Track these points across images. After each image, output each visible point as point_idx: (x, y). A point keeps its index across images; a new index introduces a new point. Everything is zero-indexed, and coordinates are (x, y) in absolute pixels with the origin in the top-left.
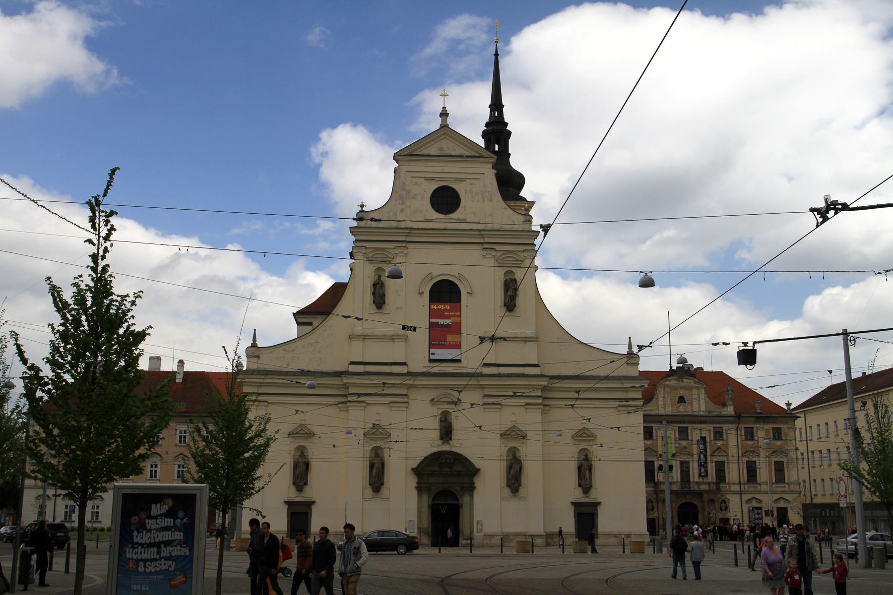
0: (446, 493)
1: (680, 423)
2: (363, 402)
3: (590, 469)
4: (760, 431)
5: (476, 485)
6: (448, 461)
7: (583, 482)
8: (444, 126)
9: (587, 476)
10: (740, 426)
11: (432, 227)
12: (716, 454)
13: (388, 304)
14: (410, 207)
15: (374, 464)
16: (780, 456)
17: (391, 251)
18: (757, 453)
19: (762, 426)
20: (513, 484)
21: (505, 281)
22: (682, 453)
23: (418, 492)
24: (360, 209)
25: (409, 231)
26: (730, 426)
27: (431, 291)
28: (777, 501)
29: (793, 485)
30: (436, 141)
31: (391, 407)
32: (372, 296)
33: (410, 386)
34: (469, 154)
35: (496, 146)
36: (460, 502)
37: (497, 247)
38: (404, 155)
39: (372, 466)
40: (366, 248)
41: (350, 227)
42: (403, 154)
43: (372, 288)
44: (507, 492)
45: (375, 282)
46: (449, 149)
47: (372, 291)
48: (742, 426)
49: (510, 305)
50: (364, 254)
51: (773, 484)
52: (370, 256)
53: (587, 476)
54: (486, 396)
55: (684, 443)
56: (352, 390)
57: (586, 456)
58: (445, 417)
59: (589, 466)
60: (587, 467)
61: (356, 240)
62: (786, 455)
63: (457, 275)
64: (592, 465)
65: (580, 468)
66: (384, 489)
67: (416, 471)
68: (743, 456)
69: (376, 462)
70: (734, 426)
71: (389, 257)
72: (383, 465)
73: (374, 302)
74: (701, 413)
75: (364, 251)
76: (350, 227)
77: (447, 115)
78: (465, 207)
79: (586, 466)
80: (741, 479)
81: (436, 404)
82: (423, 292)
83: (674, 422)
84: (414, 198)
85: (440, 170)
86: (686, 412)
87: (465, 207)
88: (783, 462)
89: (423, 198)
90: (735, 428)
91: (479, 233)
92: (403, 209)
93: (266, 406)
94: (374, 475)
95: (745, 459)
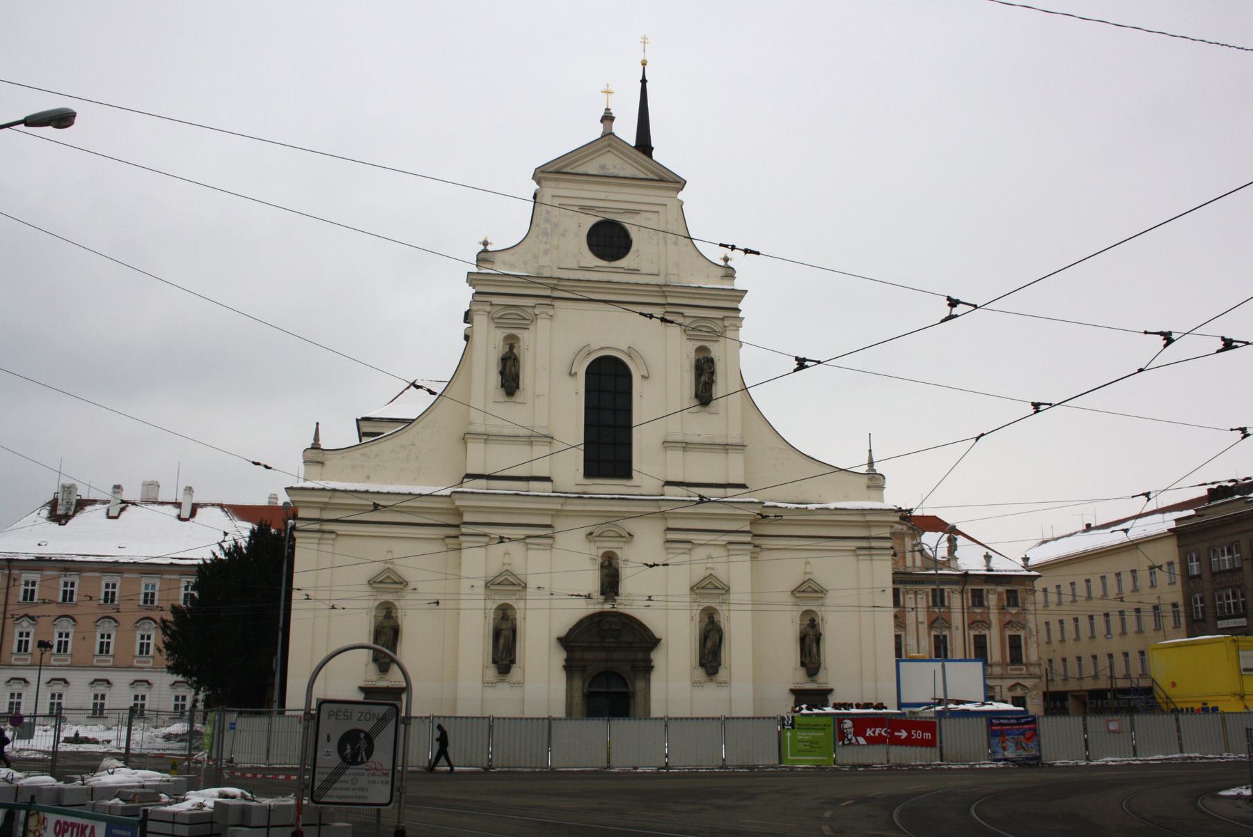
0: (609, 675)
2: (485, 535)
3: (818, 638)
5: (653, 663)
6: (613, 627)
7: (807, 661)
8: (608, 134)
9: (815, 649)
10: (965, 588)
11: (591, 279)
12: (935, 625)
13: (524, 389)
15: (501, 630)
16: (1015, 627)
17: (530, 310)
18: (987, 624)
19: (993, 587)
20: (710, 662)
21: (698, 361)
23: (567, 673)
25: (556, 282)
26: (954, 587)
27: (587, 373)
28: (1011, 688)
29: (1032, 667)
30: (596, 155)
31: (527, 544)
32: (500, 377)
33: (557, 513)
34: (644, 176)
36: (631, 690)
37: (687, 311)
38: (550, 172)
39: (497, 634)
40: (492, 305)
41: (468, 273)
42: (549, 170)
43: (500, 364)
44: (700, 673)
45: (504, 355)
46: (614, 167)
47: (500, 369)
48: (969, 587)
49: (704, 395)
50: (489, 313)
51: (1007, 665)
52: (498, 316)
53: (815, 649)
54: (669, 529)
56: (467, 518)
57: (813, 620)
58: (609, 561)
59: (815, 635)
60: (814, 637)
61: (477, 293)
62: (1023, 627)
63: (625, 348)
64: (820, 635)
65: (803, 639)
66: (515, 671)
67: (566, 642)
68: (970, 628)
69: (504, 627)
70: (958, 588)
71: (525, 319)
72: (514, 631)
73: (503, 386)
75: (488, 308)
76: (468, 273)
77: (612, 119)
78: (637, 251)
79: (812, 636)
81: (595, 541)
82: (576, 373)
85: (602, 196)
87: (637, 251)
88: (1019, 636)
89: (576, 235)
90: (960, 590)
91: (660, 290)
92: (548, 250)
93: (333, 540)
94: (501, 647)
95: (973, 633)
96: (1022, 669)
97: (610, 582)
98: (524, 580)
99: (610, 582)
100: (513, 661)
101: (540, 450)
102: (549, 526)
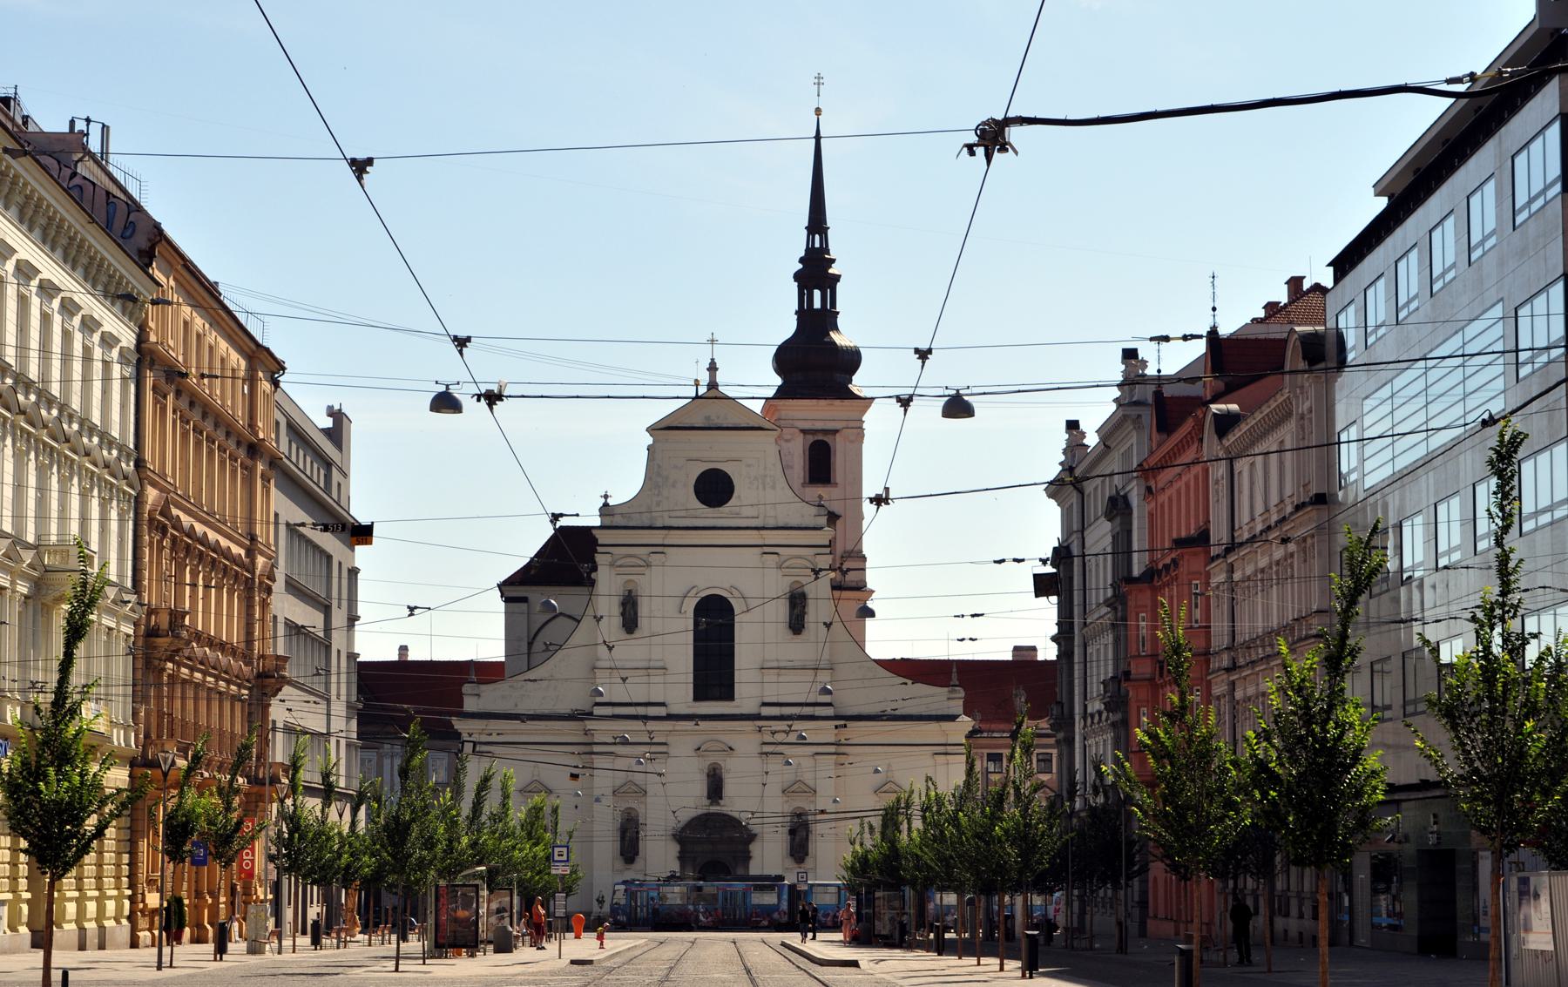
8: (713, 385)
14: (667, 498)
24: (603, 500)
35: (817, 294)
47: (621, 610)
63: (727, 586)
84: (674, 486)
87: (739, 497)
97: (715, 787)
98: (644, 787)
99: (715, 787)
100: (637, 853)
101: (657, 679)
102: (665, 744)
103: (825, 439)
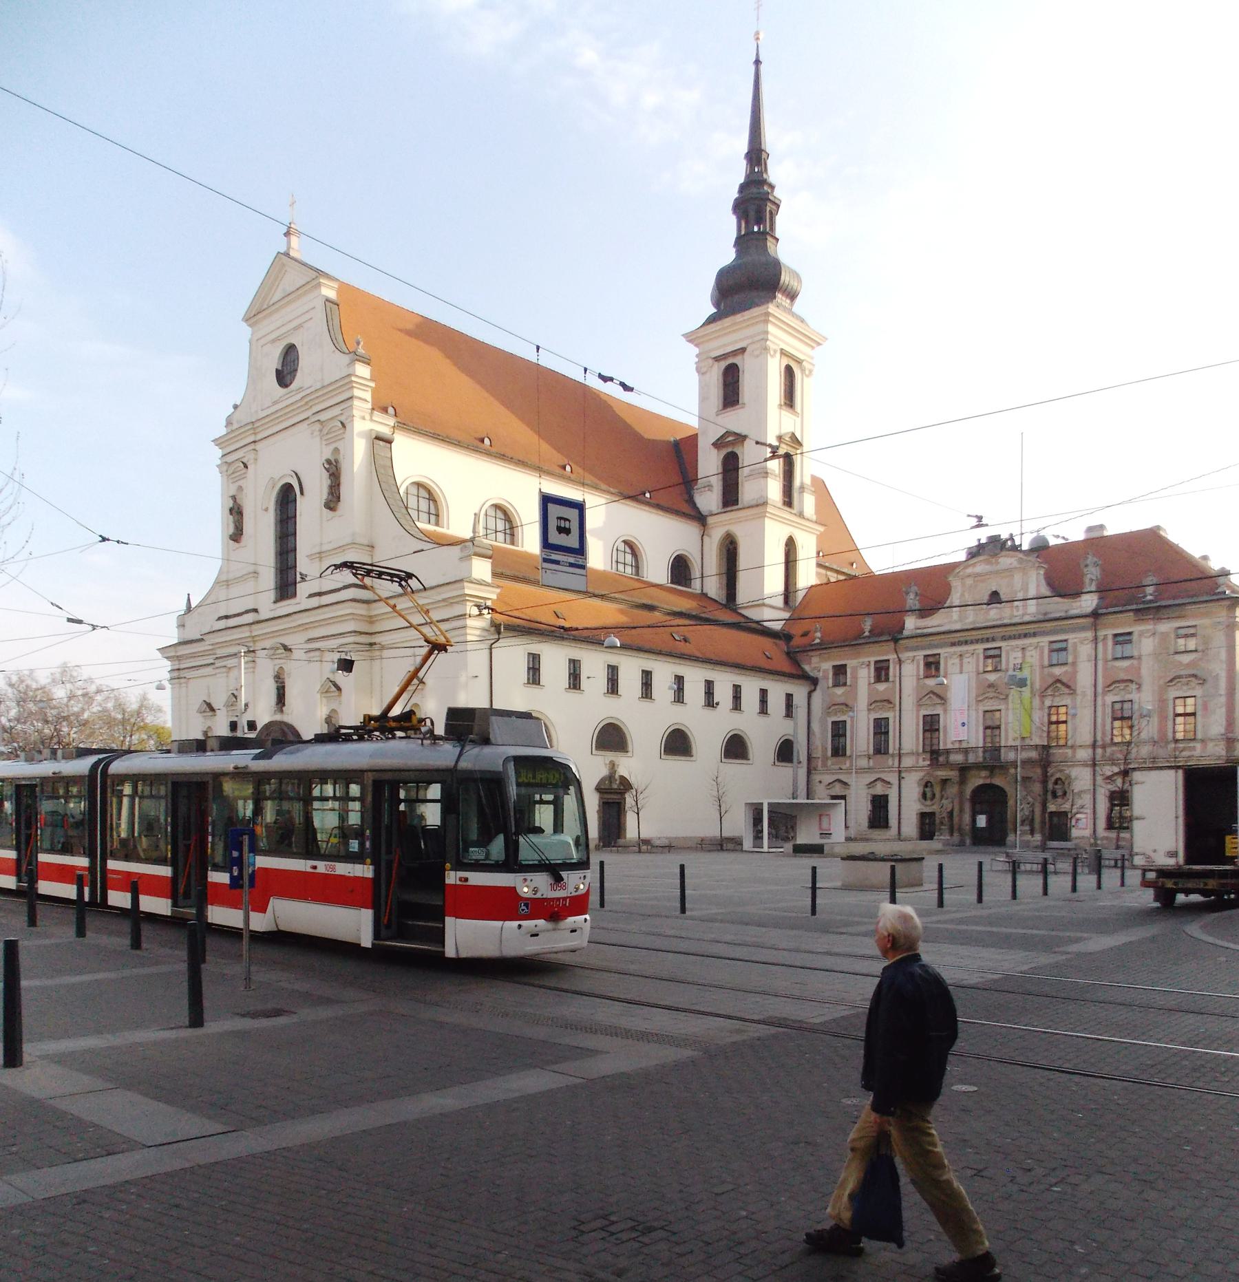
1: (988, 640)
4: (1146, 637)
22: (986, 695)
55: (992, 677)
70: (1089, 635)
74: (1027, 619)
80: (1099, 738)
83: (977, 641)
86: (1000, 619)
95: (1110, 698)
96: (1194, 748)
103: (736, 360)
